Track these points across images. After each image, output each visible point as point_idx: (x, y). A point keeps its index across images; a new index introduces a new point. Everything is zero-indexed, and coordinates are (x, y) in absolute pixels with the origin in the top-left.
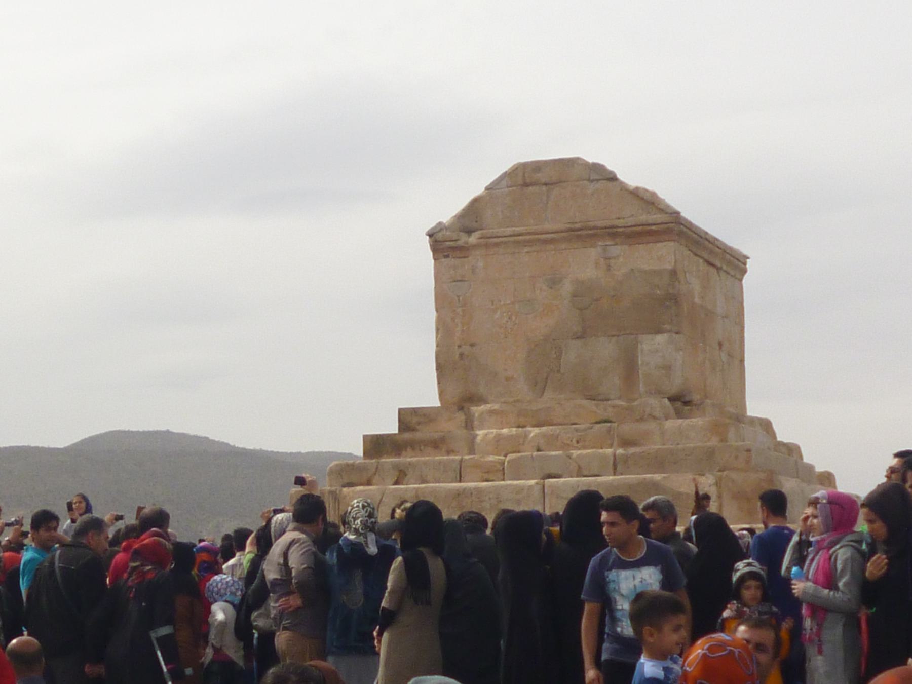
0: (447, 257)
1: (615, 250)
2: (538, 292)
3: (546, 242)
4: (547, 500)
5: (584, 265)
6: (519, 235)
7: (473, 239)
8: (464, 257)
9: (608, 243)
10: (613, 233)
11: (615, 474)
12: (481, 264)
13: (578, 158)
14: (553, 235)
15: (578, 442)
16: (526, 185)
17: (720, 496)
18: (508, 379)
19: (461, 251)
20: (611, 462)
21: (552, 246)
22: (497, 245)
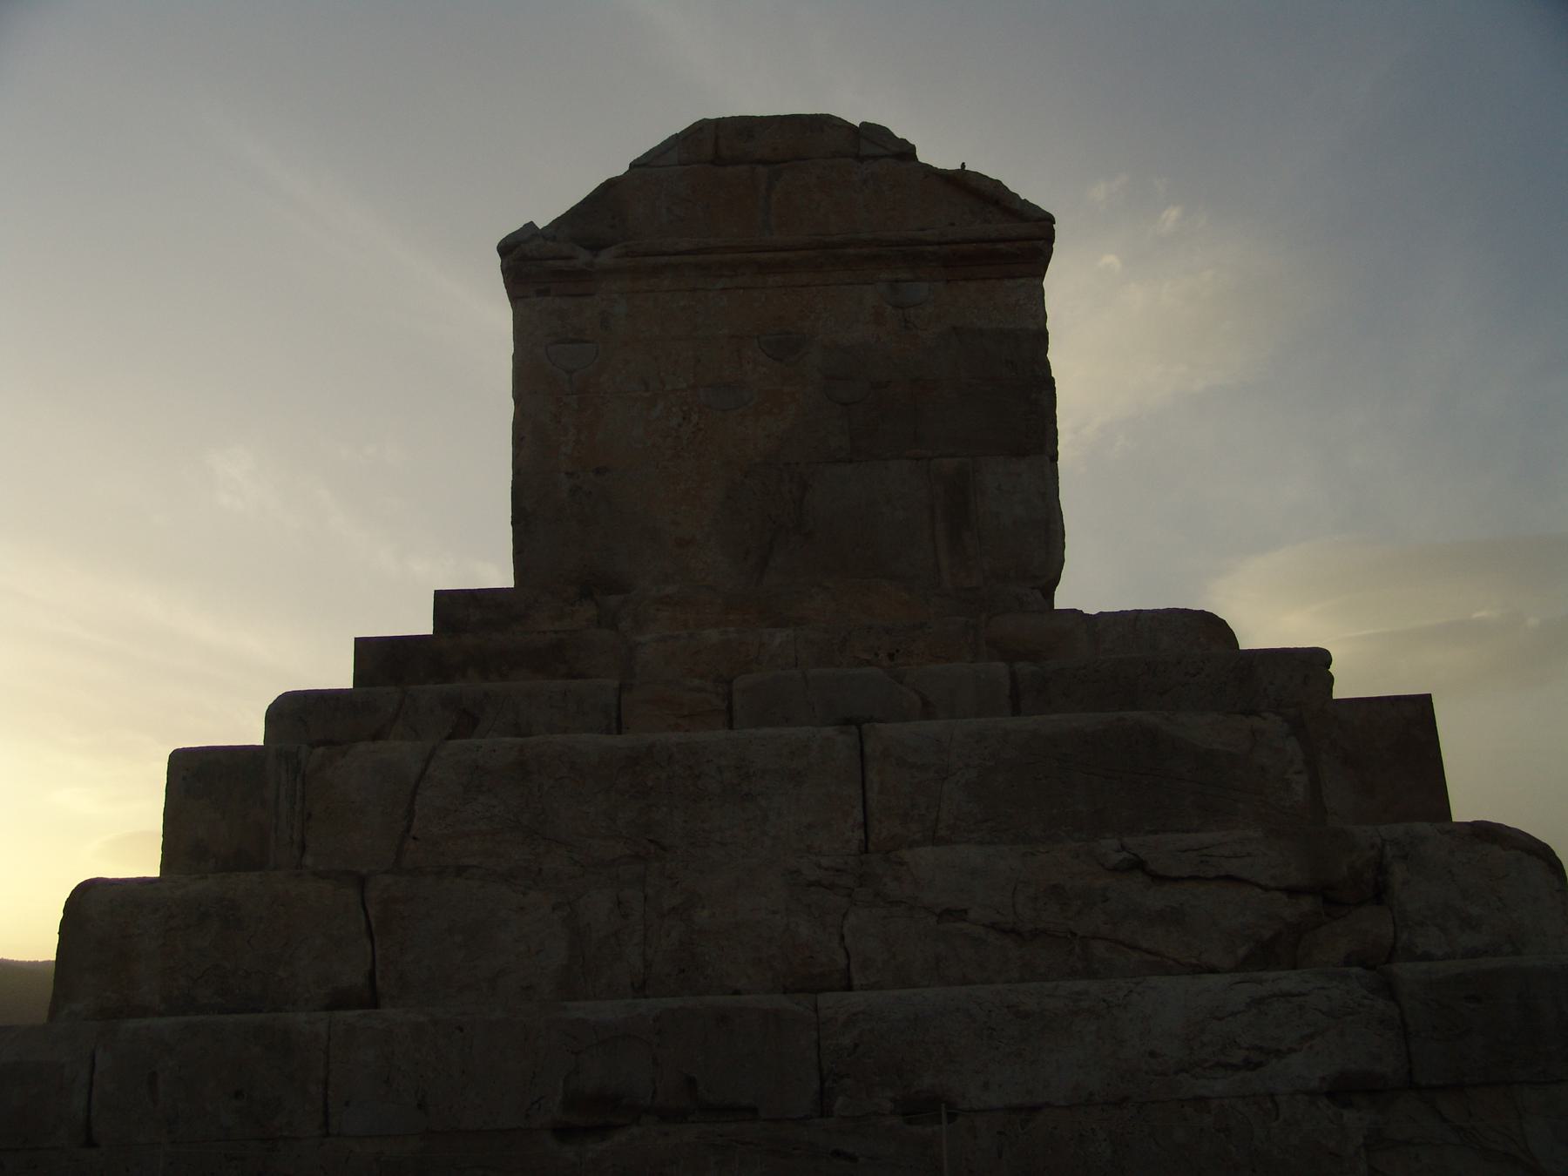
0: (543, 293)
7: (605, 258)
13: (829, 117)
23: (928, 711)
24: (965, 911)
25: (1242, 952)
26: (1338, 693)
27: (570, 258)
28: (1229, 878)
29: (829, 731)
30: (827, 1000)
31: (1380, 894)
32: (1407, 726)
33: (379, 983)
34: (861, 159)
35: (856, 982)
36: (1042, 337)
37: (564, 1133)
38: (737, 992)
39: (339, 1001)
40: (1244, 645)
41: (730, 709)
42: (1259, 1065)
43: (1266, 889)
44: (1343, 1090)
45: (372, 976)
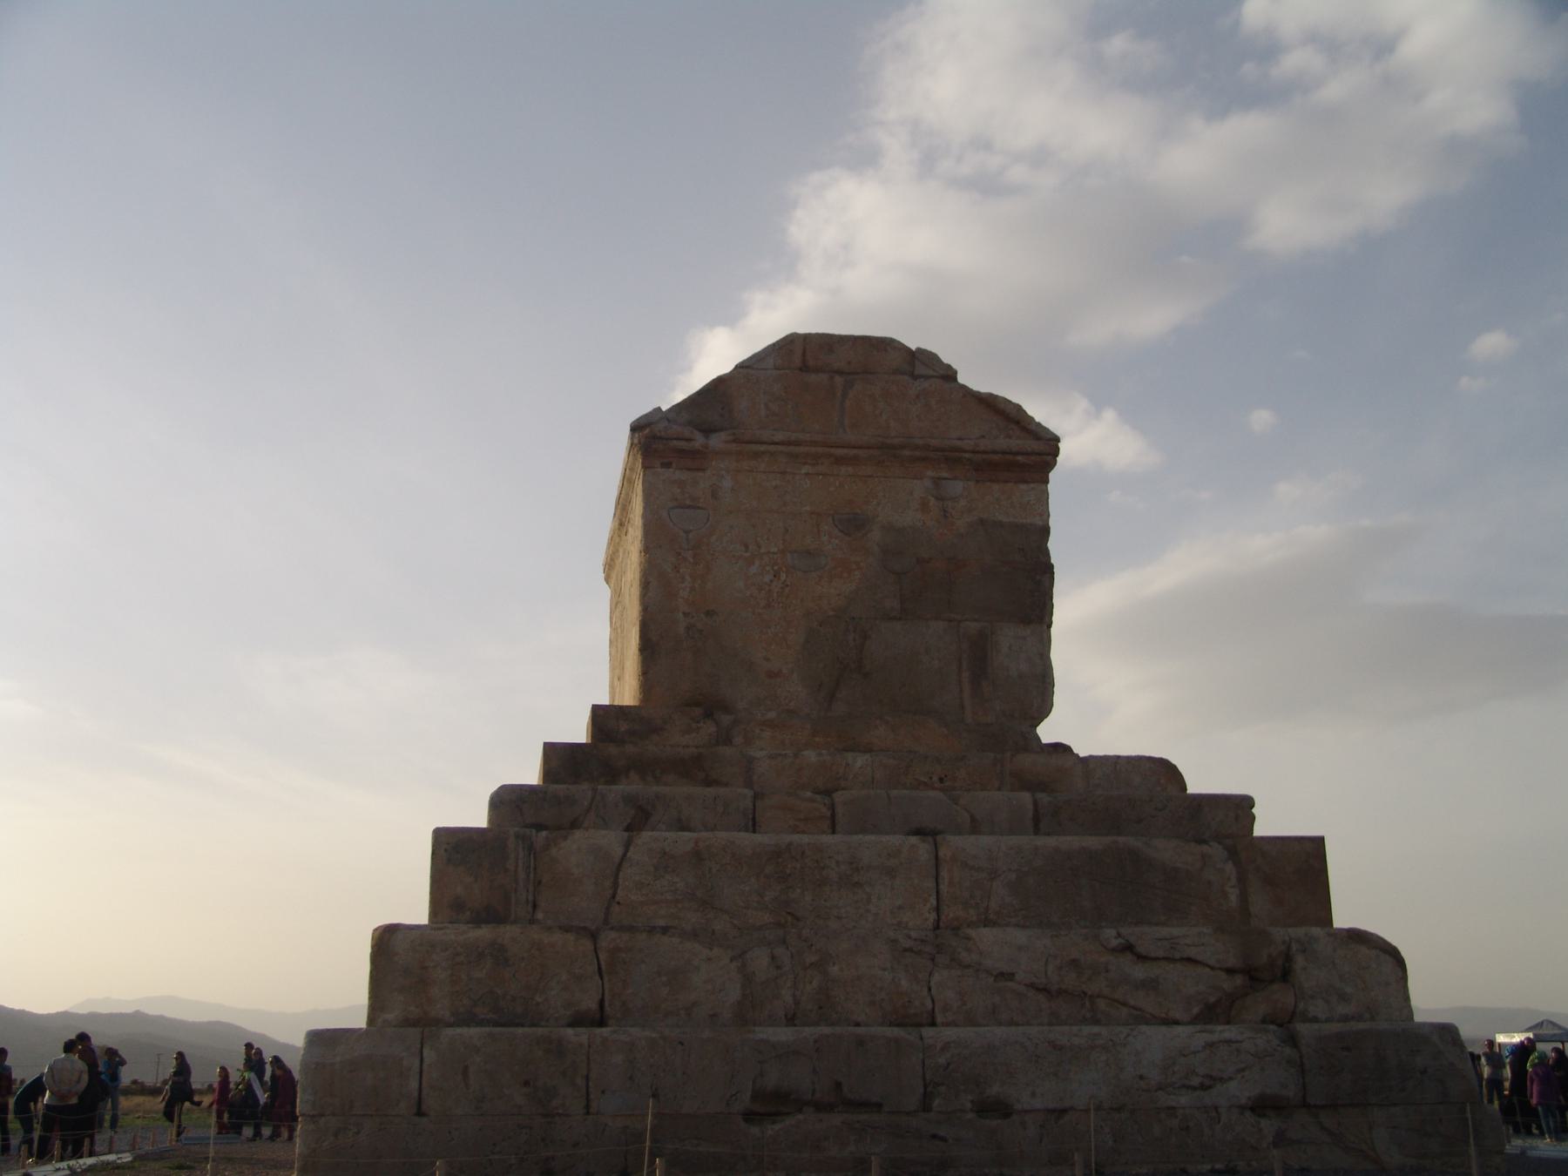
0: (664, 465)
1: (956, 487)
2: (825, 539)
3: (839, 461)
4: (944, 874)
5: (902, 503)
6: (797, 443)
7: (717, 441)
8: (698, 470)
9: (945, 475)
10: (951, 458)
11: (1037, 831)
12: (727, 483)
14: (855, 451)
15: (941, 780)
16: (804, 368)
17: (1242, 881)
18: (771, 675)
19: (694, 458)
20: (1030, 814)
21: (850, 469)
22: (756, 455)
23: (975, 828)
24: (1013, 974)
25: (1196, 1010)
26: (1259, 831)
27: (689, 440)
28: (1189, 960)
29: (914, 839)
30: (928, 1032)
31: (1286, 975)
32: (1305, 861)
33: (607, 1009)
34: (915, 377)
35: (939, 1019)
36: (1045, 531)
37: (749, 1116)
38: (858, 1025)
39: (578, 1021)
40: (1193, 788)
41: (833, 816)
42: (1210, 1087)
43: (1212, 968)
44: (1262, 1106)
45: (601, 1003)
